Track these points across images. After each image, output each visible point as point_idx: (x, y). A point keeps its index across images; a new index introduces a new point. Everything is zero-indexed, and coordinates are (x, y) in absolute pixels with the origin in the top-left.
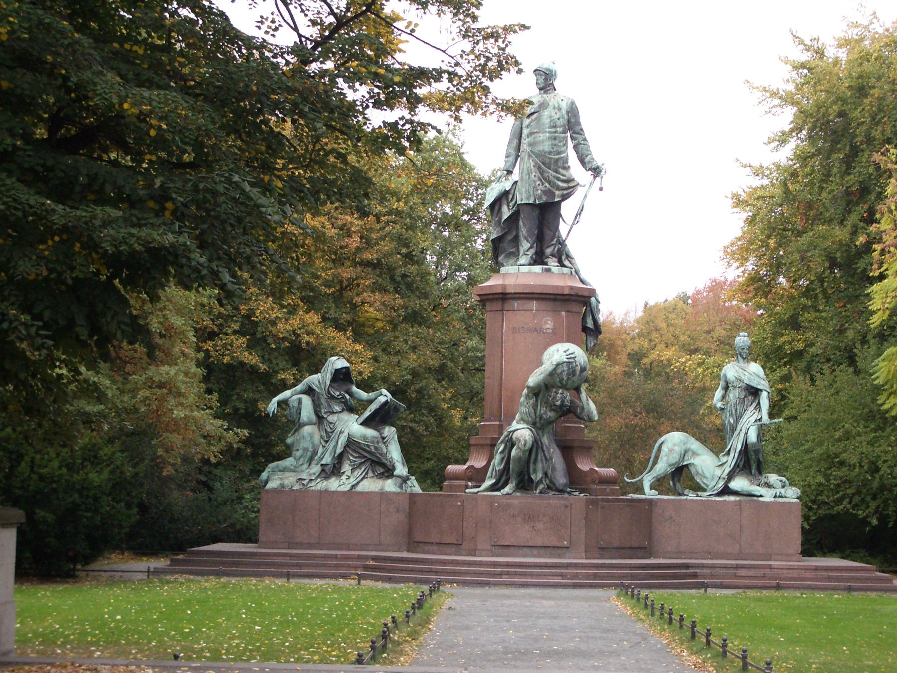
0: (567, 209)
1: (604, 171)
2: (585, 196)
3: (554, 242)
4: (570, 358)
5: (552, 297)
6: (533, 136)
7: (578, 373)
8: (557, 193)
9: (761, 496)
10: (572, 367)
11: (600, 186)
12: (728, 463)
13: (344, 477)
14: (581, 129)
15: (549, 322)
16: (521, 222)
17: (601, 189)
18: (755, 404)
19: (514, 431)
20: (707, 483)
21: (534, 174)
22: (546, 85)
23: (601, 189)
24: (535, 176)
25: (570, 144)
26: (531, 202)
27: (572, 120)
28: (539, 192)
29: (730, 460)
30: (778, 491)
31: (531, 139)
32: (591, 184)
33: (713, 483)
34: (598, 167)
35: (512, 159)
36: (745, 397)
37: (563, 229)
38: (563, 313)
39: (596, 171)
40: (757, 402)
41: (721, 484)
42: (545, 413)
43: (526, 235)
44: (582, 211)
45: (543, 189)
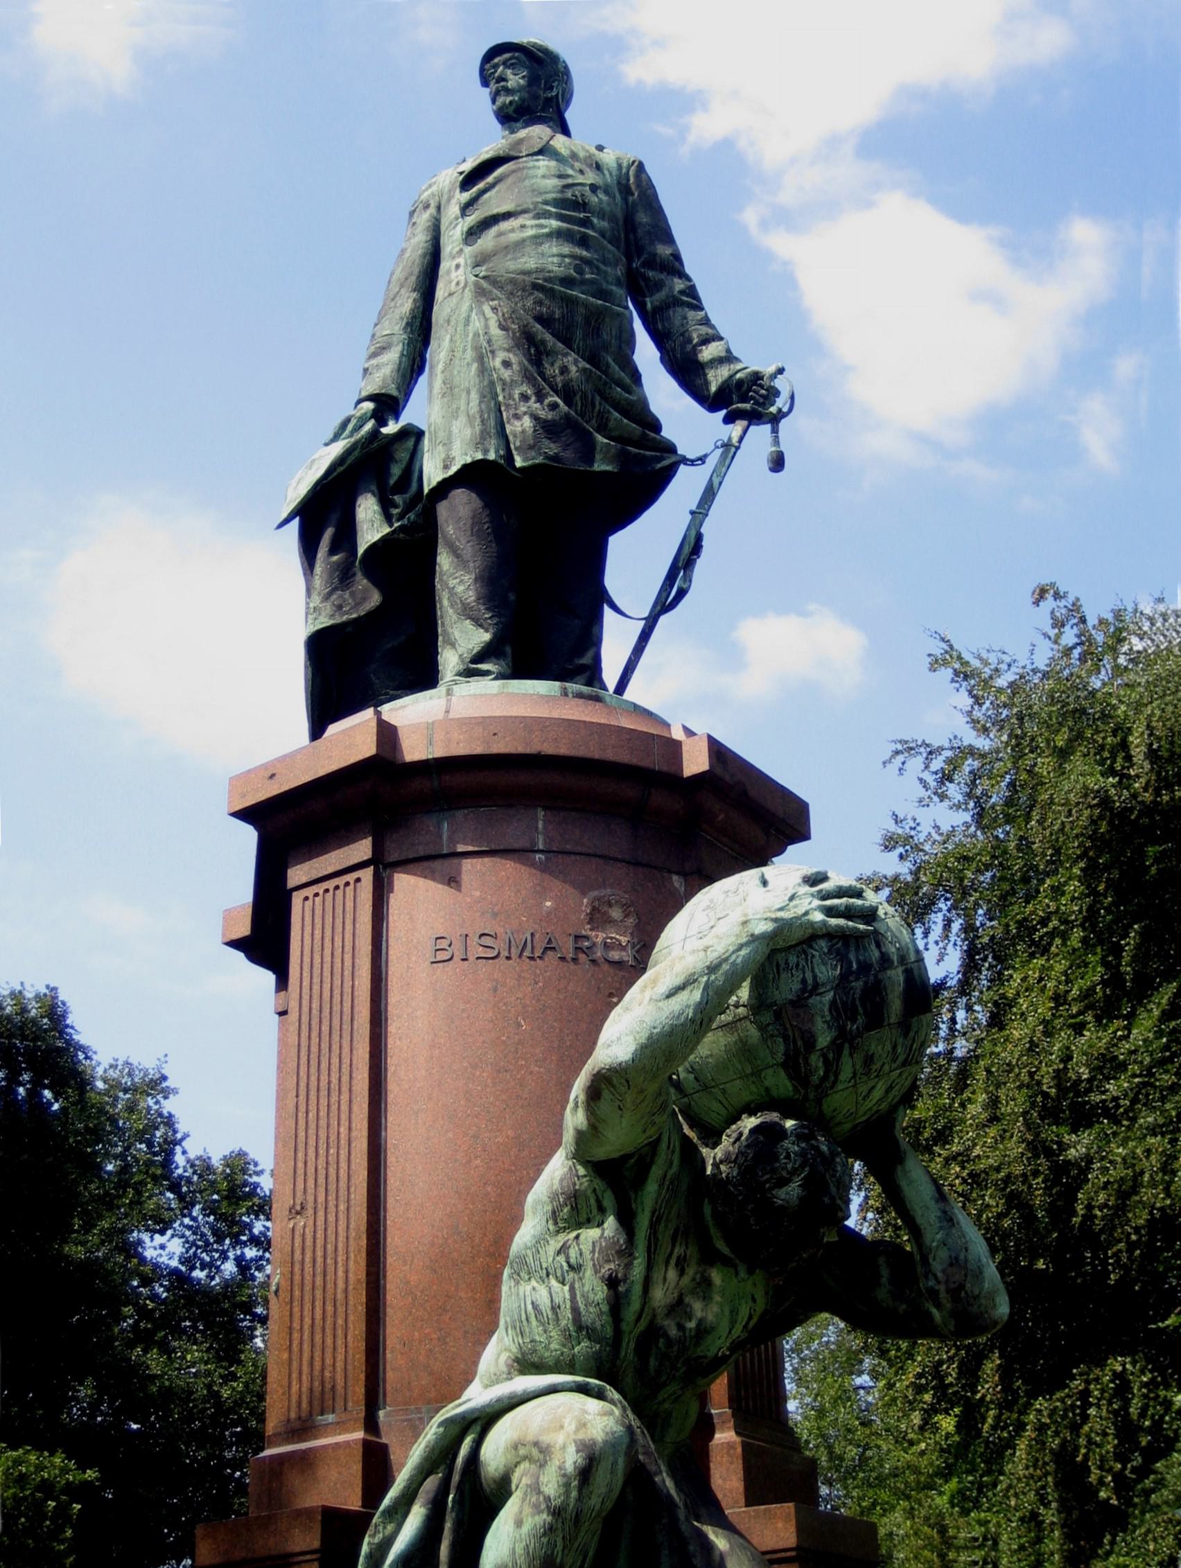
2: (709, 494)
4: (848, 913)
6: (493, 231)
7: (895, 1006)
8: (600, 438)
10: (865, 967)
14: (677, 257)
15: (616, 913)
16: (444, 561)
17: (778, 463)
19: (486, 1419)
21: (501, 356)
22: (535, 97)
23: (778, 463)
24: (506, 364)
26: (492, 456)
27: (643, 218)
28: (527, 422)
31: (488, 240)
34: (757, 377)
35: (393, 356)
42: (678, 1307)
43: (471, 597)
44: (697, 549)
45: (544, 414)
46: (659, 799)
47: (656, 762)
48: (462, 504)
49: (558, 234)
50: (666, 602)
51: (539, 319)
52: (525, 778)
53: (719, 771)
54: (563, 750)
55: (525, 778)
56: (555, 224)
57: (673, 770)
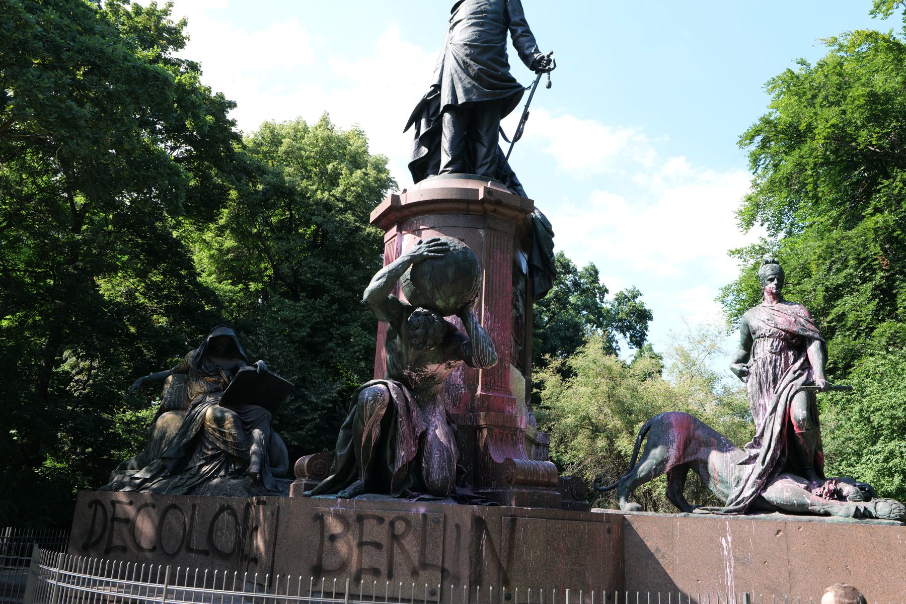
0: (509, 124)
1: (552, 63)
3: (489, 159)
5: (464, 206)
9: (827, 514)
11: (547, 84)
12: (759, 459)
13: (188, 475)
17: (549, 86)
18: (802, 360)
20: (725, 491)
23: (549, 86)
25: (509, 41)
29: (765, 451)
30: (862, 505)
32: (536, 83)
33: (736, 491)
34: (543, 57)
36: (782, 350)
37: (504, 146)
38: (481, 232)
39: (540, 66)
40: (802, 360)
41: (748, 493)
46: (472, 207)
47: (471, 198)
48: (447, 117)
49: (472, 25)
50: (518, 135)
51: (467, 55)
52: (431, 207)
53: (488, 197)
54: (440, 197)
55: (431, 207)
56: (474, 21)
57: (474, 198)
